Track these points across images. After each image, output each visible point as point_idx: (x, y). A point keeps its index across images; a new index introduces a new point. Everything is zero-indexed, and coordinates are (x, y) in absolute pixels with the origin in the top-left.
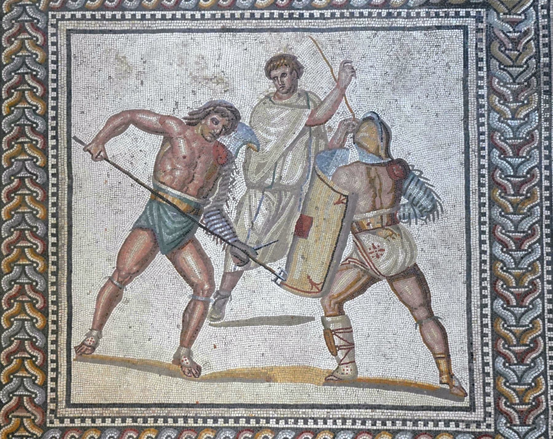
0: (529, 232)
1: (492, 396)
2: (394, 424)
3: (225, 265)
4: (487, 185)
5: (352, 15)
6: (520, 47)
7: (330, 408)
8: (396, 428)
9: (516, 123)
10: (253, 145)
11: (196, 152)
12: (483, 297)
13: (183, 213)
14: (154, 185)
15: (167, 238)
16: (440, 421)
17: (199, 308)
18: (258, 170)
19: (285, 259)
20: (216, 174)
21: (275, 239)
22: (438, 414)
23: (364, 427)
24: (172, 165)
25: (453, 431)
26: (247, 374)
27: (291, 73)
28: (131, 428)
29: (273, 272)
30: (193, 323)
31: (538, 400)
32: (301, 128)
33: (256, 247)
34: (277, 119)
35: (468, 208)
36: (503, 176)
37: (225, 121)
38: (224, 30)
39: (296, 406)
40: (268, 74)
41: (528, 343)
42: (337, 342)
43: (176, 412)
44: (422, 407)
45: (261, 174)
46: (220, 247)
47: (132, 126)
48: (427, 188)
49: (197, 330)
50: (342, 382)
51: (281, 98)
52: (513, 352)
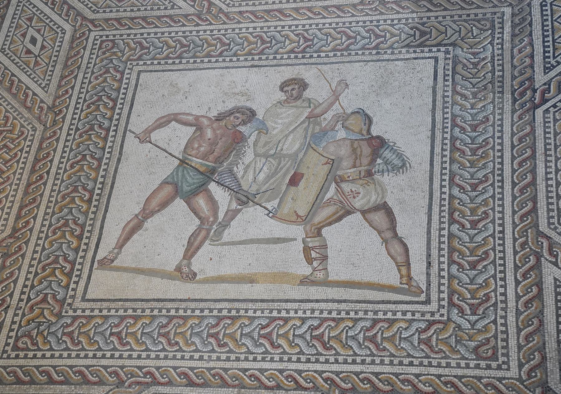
0: (483, 179)
1: (446, 293)
2: (356, 313)
3: (229, 205)
4: (449, 150)
5: (350, 54)
6: (479, 67)
7: (302, 302)
8: (358, 317)
9: (475, 111)
10: (263, 129)
11: (219, 136)
12: (441, 223)
13: (202, 173)
14: (183, 157)
15: (186, 188)
16: (398, 311)
17: (203, 233)
18: (265, 145)
19: (278, 200)
20: (232, 149)
21: (272, 187)
22: (396, 307)
23: (330, 316)
24: (199, 144)
25: (409, 319)
26: (234, 278)
27: (299, 88)
28: (130, 317)
29: (267, 209)
30: (196, 244)
31: (488, 295)
32: (302, 120)
33: (255, 193)
34: (284, 115)
35: (432, 165)
36: (462, 144)
37: (244, 117)
38: (252, 66)
39: (273, 301)
40: (281, 89)
41: (480, 254)
42: (314, 255)
43: (169, 305)
44: (383, 301)
45: (267, 148)
46: (227, 194)
47: (173, 123)
48: (399, 153)
49: (198, 248)
50: (314, 283)
51: (289, 103)
52: (466, 261)
